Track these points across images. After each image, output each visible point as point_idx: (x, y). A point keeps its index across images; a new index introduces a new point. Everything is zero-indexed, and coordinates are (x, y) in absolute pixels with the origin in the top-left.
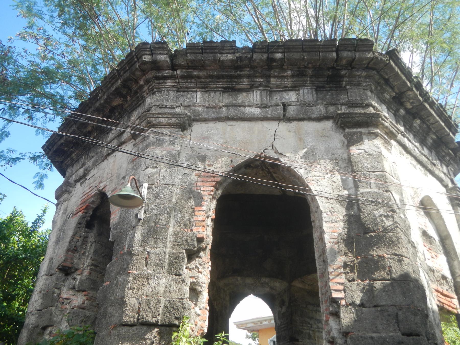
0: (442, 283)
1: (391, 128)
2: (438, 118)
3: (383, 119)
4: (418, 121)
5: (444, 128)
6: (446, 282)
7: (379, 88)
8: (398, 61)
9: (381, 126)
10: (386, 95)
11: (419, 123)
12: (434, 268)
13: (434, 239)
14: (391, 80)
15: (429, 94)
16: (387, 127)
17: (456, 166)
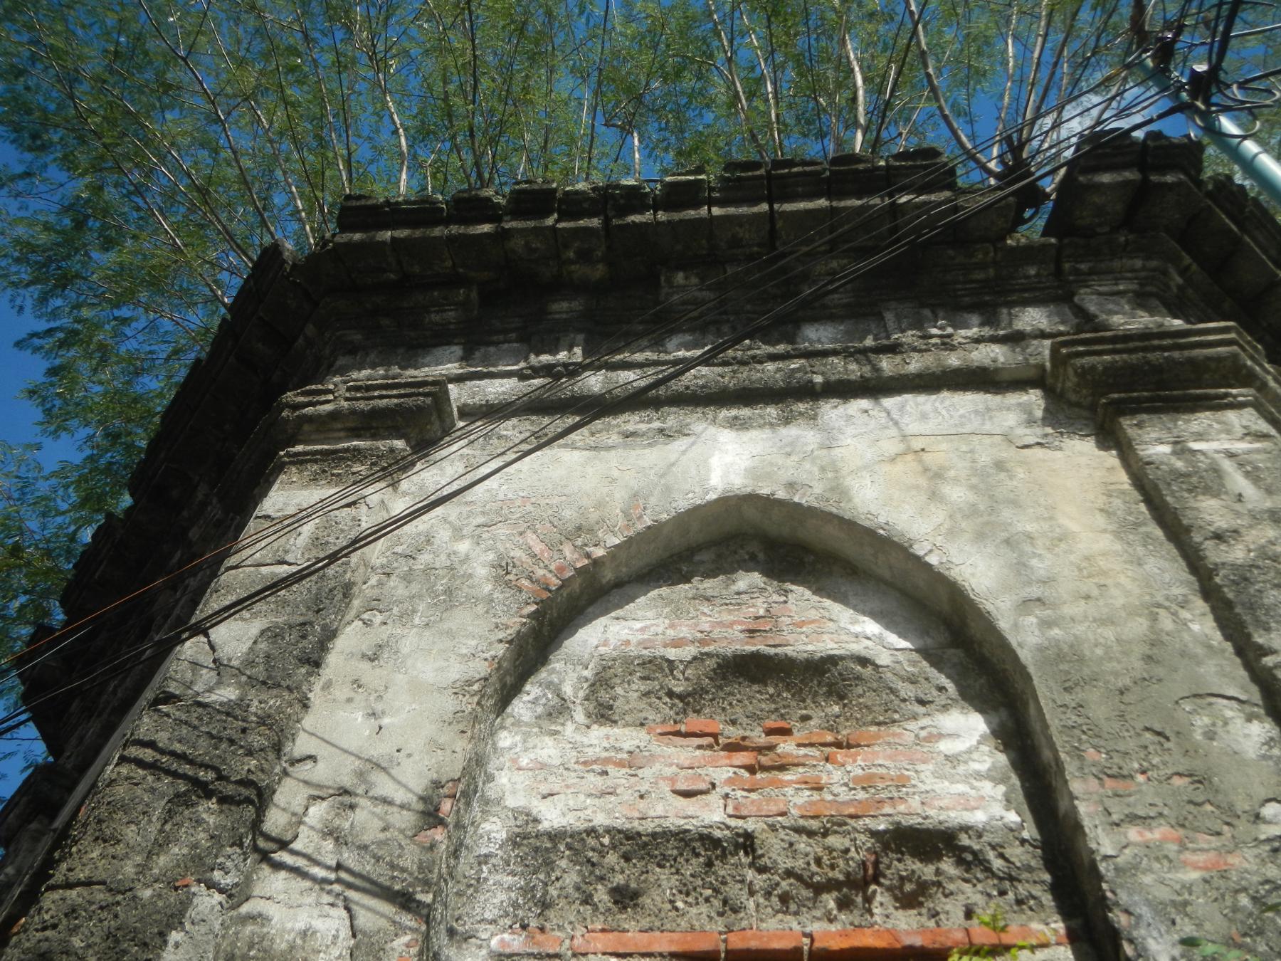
0: (923, 888)
1: (362, 405)
2: (764, 207)
3: (296, 407)
4: (680, 278)
5: (832, 211)
6: (960, 862)
7: (385, 322)
8: (391, 214)
9: (306, 427)
10: (435, 318)
11: (694, 280)
12: (750, 825)
13: (864, 661)
14: (417, 269)
15: (618, 186)
16: (335, 415)
17: (1138, 263)
